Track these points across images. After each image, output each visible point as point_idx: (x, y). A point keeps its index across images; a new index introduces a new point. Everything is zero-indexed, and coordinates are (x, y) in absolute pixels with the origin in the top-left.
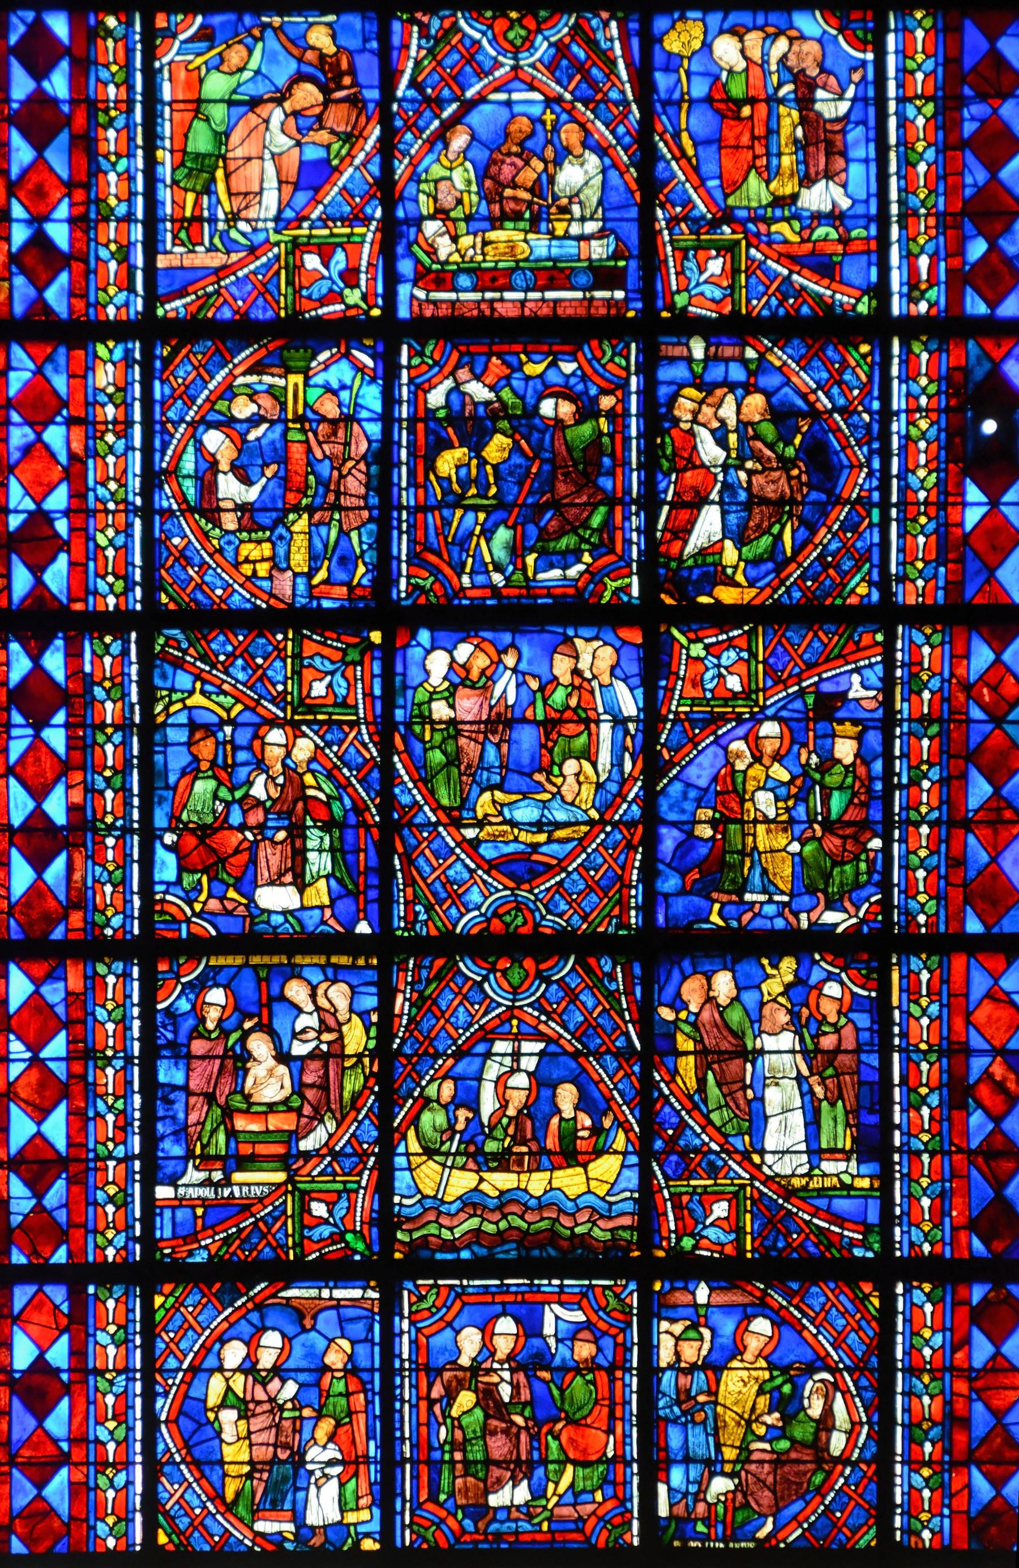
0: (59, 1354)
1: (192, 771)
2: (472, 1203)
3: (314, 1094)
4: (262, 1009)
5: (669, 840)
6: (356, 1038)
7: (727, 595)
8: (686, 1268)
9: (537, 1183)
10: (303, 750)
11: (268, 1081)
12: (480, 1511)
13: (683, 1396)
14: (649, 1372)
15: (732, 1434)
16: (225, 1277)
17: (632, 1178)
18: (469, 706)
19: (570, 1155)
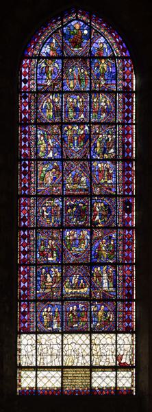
0: (26, 310)
1: (41, 245)
2: (71, 293)
3: (54, 281)
4: (48, 271)
5: (93, 252)
6: (59, 275)
7: (99, 225)
8: (95, 300)
9: (78, 291)
10: (53, 242)
11: (49, 279)
12: (72, 327)
13: (94, 314)
14: (91, 312)
15: (100, 319)
16: (45, 301)
17: (89, 290)
18: (71, 238)
19: (82, 288)
